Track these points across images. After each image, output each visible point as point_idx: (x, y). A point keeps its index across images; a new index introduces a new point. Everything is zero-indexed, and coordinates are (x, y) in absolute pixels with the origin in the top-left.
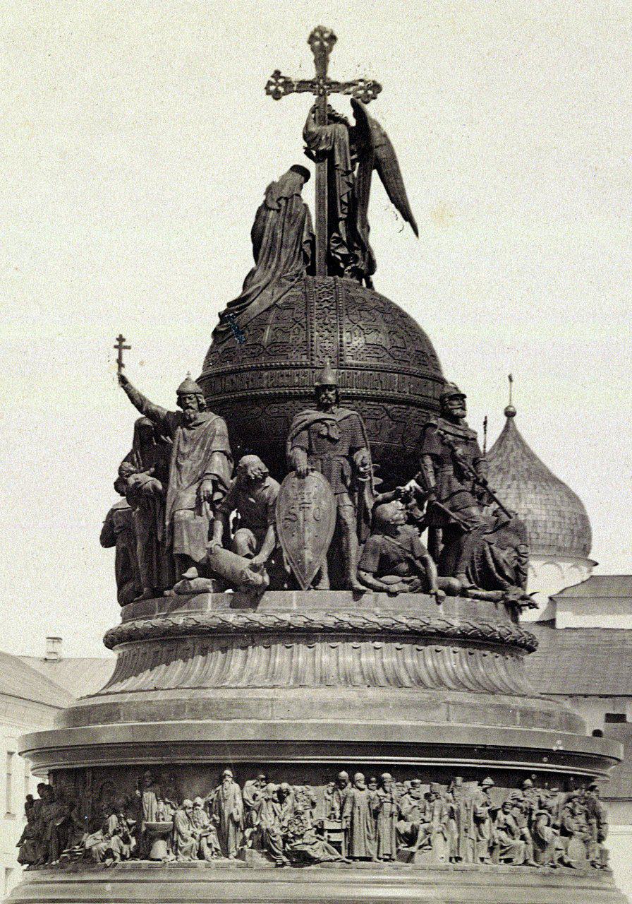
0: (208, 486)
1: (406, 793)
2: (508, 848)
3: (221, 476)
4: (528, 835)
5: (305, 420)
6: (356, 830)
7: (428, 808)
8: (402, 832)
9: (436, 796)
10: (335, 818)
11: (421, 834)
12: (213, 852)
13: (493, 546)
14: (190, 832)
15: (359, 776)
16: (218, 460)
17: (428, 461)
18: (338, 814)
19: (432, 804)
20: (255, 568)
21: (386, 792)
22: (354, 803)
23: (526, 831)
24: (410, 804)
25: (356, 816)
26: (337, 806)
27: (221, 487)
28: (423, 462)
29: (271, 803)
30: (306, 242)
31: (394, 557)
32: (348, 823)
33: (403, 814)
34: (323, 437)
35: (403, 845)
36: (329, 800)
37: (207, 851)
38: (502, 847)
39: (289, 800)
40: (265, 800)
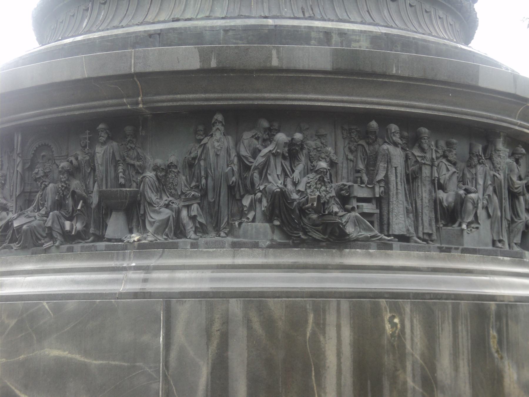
6: (393, 199)
7: (468, 176)
8: (445, 204)
9: (479, 161)
10: (362, 182)
11: (470, 206)
12: (196, 228)
14: (162, 203)
15: (394, 127)
18: (365, 179)
19: (473, 171)
24: (448, 170)
25: (392, 178)
26: (361, 166)
29: (279, 160)
32: (382, 189)
33: (442, 182)
37: (190, 226)
40: (273, 154)
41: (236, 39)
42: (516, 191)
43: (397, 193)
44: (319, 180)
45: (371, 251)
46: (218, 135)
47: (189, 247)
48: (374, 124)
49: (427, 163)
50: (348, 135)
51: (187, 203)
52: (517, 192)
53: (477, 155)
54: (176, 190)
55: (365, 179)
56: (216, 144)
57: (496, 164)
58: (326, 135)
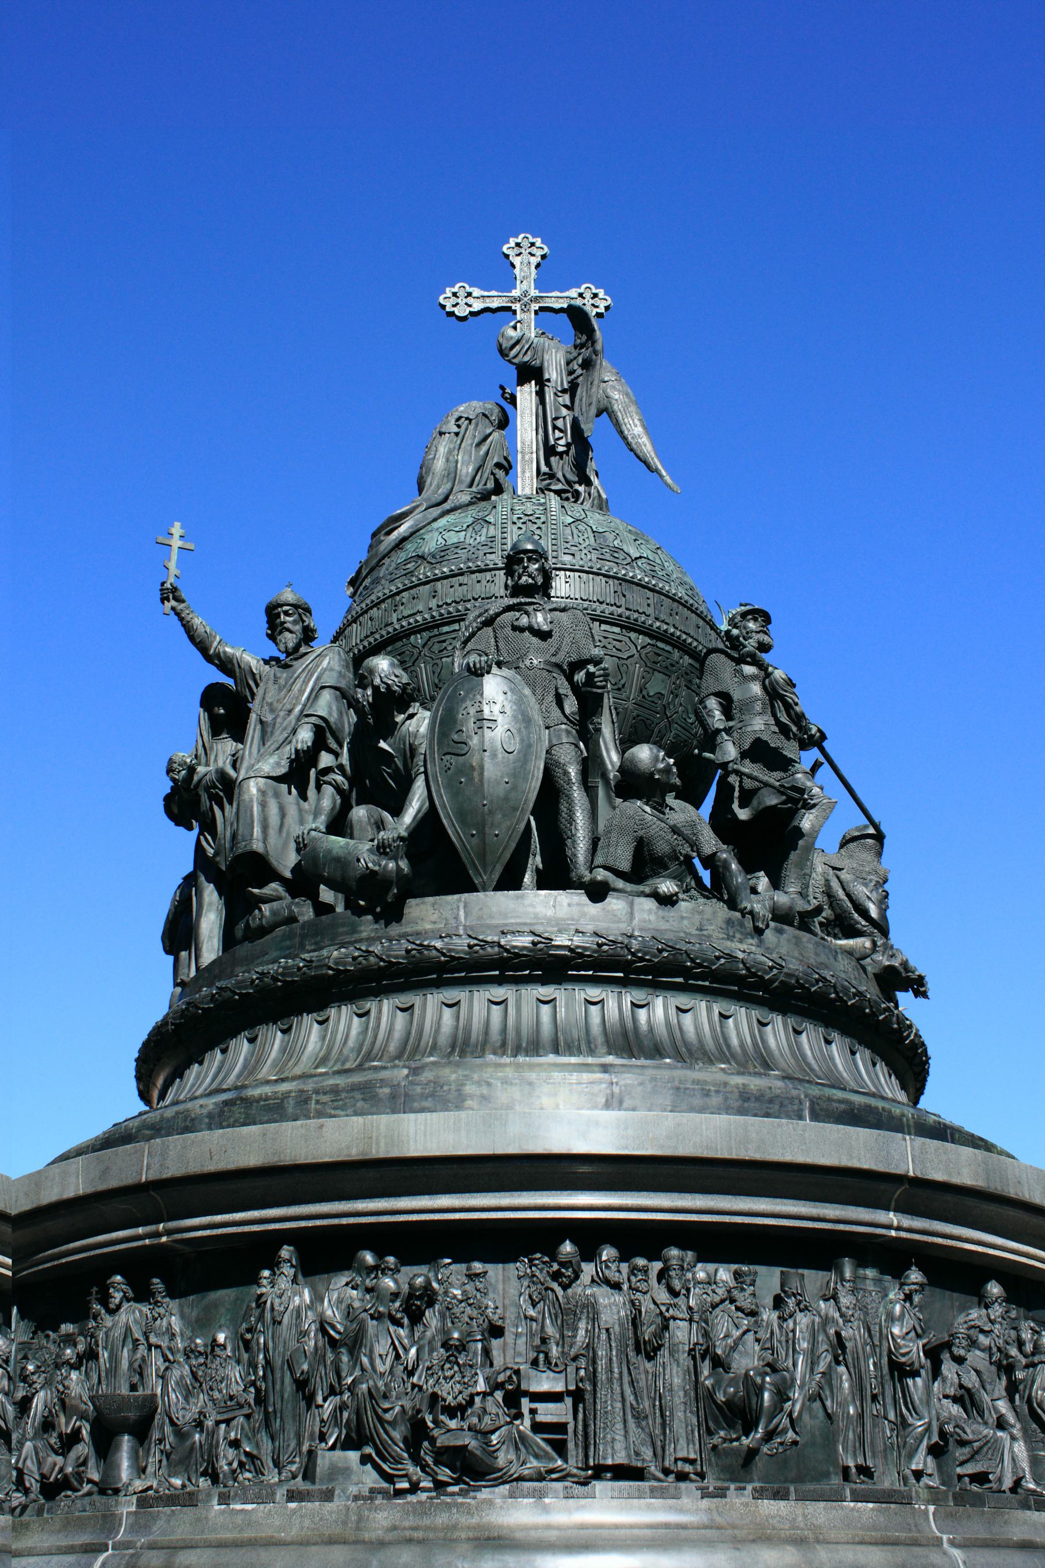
0: (305, 736)
1: (722, 1301)
2: (976, 1445)
3: (332, 720)
4: (1011, 1418)
5: (487, 611)
9: (798, 1304)
13: (844, 875)
16: (327, 696)
17: (713, 703)
20: (382, 849)
21: (674, 1294)
22: (594, 1318)
23: (1003, 1406)
26: (550, 1330)
27: (333, 745)
28: (705, 707)
30: (498, 465)
31: (662, 848)
32: (582, 1373)
34: (522, 630)
35: (722, 1433)
36: (532, 1319)
38: (962, 1443)
39: (432, 1318)
41: (335, 1108)
42: (903, 1360)
43: (610, 1380)
44: (448, 1360)
45: (547, 1500)
46: (283, 1283)
47: (215, 1501)
48: (568, 1247)
49: (681, 1316)
50: (528, 1271)
51: (225, 1416)
52: (904, 1364)
53: (794, 1295)
54: (220, 1391)
55: (555, 1351)
56: (277, 1301)
57: (844, 1309)
58: (486, 1273)
